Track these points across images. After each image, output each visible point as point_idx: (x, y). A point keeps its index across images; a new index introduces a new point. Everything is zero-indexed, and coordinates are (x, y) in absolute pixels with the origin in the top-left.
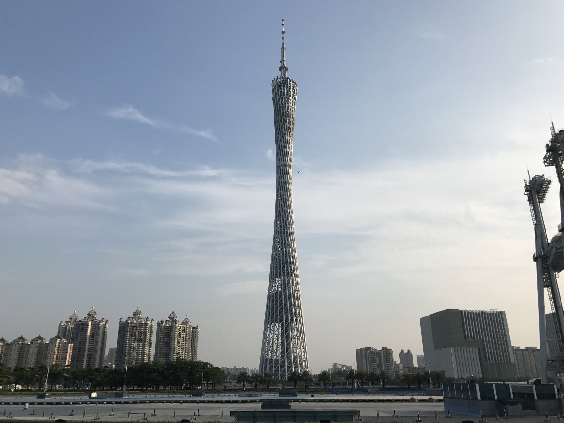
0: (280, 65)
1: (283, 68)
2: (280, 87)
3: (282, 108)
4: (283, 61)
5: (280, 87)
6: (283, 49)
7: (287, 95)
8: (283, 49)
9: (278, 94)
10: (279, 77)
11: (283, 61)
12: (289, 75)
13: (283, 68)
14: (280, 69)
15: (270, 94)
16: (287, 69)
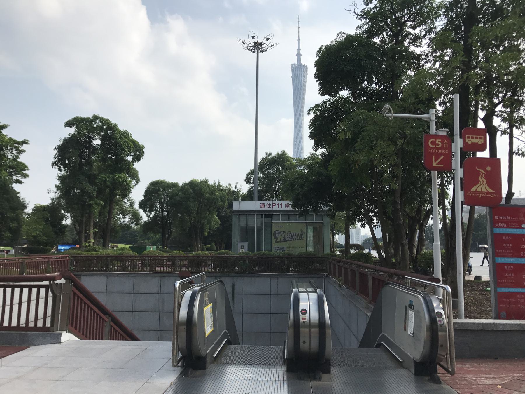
0: (296, 52)
1: (299, 55)
2: (297, 70)
3: (298, 85)
4: (299, 50)
5: (297, 70)
6: (299, 40)
7: (302, 76)
8: (299, 40)
9: (296, 76)
10: (296, 63)
11: (299, 50)
12: (303, 62)
13: (299, 55)
14: (297, 55)
15: (290, 74)
16: (301, 55)
